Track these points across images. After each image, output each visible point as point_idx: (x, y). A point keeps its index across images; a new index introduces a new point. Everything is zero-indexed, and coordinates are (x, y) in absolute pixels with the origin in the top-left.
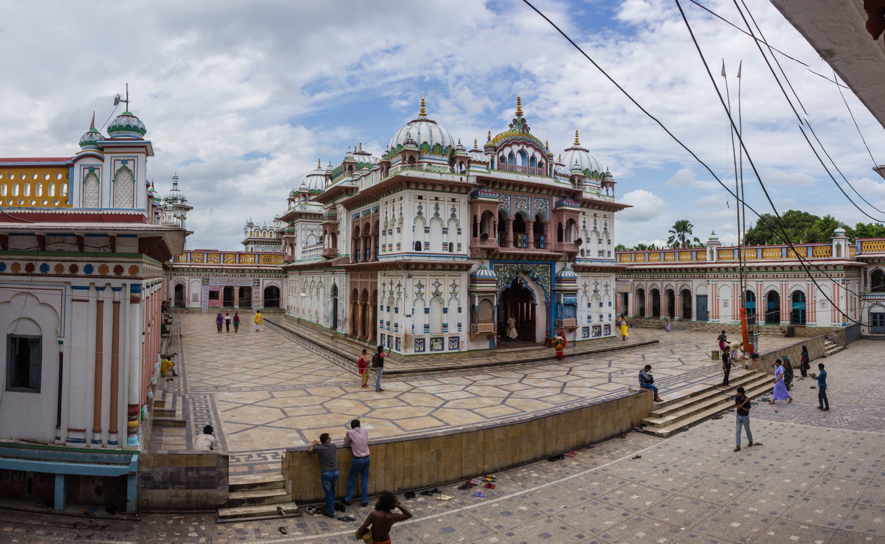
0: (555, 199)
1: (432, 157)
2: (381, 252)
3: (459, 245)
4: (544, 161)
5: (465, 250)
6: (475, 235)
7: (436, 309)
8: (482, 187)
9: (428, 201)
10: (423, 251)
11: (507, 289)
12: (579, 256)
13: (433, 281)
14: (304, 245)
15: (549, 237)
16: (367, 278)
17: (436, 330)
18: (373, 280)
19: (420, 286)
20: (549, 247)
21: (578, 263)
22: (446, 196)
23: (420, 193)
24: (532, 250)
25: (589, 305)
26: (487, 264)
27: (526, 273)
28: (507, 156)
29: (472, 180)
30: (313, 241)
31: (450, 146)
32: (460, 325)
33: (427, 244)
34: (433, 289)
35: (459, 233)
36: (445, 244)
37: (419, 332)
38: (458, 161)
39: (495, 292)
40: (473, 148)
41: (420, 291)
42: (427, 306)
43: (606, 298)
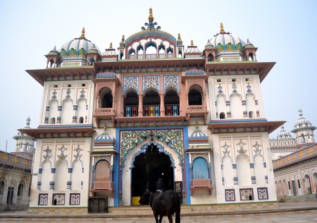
3: (86, 118)
4: (172, 47)
9: (61, 88)
11: (142, 154)
13: (60, 146)
19: (48, 150)
31: (83, 49)
33: (59, 119)
34: (59, 153)
35: (87, 109)
36: (75, 118)
37: (46, 188)
40: (108, 48)
41: (47, 155)
42: (53, 167)
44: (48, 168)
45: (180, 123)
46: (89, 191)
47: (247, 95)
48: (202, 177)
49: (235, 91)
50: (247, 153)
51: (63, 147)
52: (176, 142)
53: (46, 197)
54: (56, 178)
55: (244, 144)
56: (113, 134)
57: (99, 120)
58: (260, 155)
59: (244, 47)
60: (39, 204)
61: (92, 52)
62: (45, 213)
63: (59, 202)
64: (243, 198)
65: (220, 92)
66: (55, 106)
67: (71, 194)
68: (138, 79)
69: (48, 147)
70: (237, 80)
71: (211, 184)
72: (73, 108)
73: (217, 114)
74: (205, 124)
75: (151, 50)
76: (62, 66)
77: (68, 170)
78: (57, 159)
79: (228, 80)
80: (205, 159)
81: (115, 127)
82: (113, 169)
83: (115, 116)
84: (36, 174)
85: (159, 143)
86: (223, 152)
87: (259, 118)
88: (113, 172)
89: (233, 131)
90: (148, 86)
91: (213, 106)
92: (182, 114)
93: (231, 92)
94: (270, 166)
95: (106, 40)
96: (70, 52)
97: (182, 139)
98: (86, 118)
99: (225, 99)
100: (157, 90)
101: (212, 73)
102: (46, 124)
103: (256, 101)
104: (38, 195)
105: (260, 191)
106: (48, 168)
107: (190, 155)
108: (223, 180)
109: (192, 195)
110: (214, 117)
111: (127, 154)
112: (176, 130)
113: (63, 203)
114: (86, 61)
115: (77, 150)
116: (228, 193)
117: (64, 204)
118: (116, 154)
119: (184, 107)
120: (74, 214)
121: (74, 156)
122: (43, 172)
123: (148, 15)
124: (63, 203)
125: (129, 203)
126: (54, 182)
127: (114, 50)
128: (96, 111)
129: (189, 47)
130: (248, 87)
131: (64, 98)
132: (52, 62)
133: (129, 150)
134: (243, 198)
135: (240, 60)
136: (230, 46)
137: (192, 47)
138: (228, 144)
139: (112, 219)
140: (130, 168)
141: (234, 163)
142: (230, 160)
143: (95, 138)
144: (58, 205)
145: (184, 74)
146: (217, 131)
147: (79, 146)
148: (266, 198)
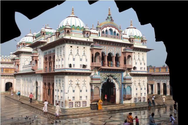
0: (123, 48)
1: (76, 31)
2: (55, 68)
4: (119, 33)
5: (89, 67)
6: (92, 61)
7: (77, 90)
8: (95, 43)
10: (72, 68)
11: (105, 82)
12: (132, 70)
14: (23, 65)
15: (121, 62)
16: (50, 78)
17: (77, 99)
18: (53, 79)
20: (121, 66)
21: (132, 72)
22: (81, 47)
23: (71, 45)
24: (114, 68)
25: (137, 89)
26: (97, 73)
27: (112, 76)
28: (105, 31)
29: (92, 41)
30: (27, 63)
31: (83, 27)
32: (86, 97)
38: (86, 33)
39: (100, 84)
41: (71, 84)
42: (74, 90)
43: (144, 86)
48: (129, 94)
49: (139, 58)
58: (144, 85)
60: (69, 107)
72: (80, 60)
84: (67, 93)
93: (138, 59)
103: (144, 63)
106: (71, 90)
113: (79, 106)
126: (74, 97)
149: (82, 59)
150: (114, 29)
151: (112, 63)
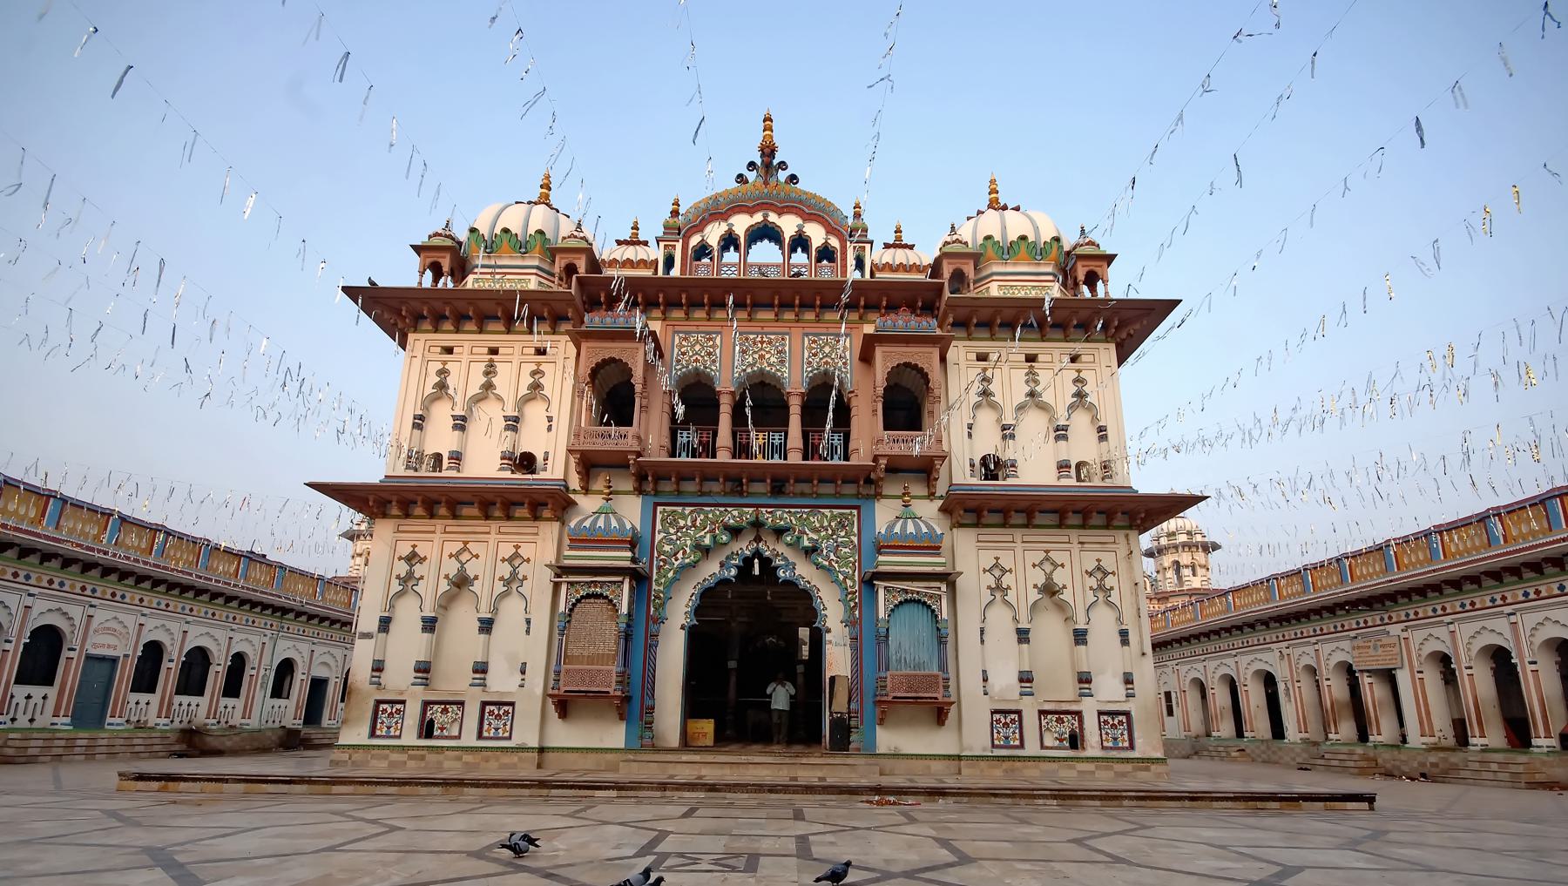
3: (546, 459)
4: (834, 242)
9: (465, 358)
11: (724, 582)
31: (540, 232)
33: (457, 457)
34: (452, 568)
35: (550, 428)
41: (410, 575)
42: (429, 613)
44: (409, 615)
45: (849, 489)
46: (546, 695)
47: (1071, 407)
48: (917, 666)
49: (1032, 394)
50: (1066, 596)
51: (465, 549)
52: (836, 550)
53: (398, 711)
54: (436, 649)
55: (1055, 565)
56: (631, 511)
57: (590, 464)
59: (1068, 253)
60: (373, 734)
61: (572, 243)
62: (392, 765)
63: (442, 729)
64: (1049, 740)
65: (985, 393)
66: (442, 415)
67: (484, 704)
68: (718, 341)
69: (414, 546)
70: (1041, 358)
71: (946, 687)
73: (972, 465)
74: (931, 496)
75: (765, 253)
76: (470, 282)
77: (478, 624)
78: (444, 586)
79: (1012, 357)
80: (929, 607)
81: (639, 491)
82: (628, 626)
83: (639, 454)
84: (368, 636)
85: (781, 548)
86: (989, 587)
87: (1108, 483)
88: (627, 636)
89: (1025, 521)
90: (752, 365)
91: (962, 436)
92: (861, 456)
93: (1021, 398)
94: (1142, 636)
95: (622, 211)
96: (498, 241)
97: (855, 539)
98: (546, 459)
99: (999, 420)
100: (778, 379)
101: (962, 333)
102: (411, 473)
103: (1101, 429)
104: (372, 704)
105: (1106, 722)
106: (409, 615)
107: (881, 593)
108: (986, 680)
109: (881, 722)
110: (961, 473)
111: (675, 579)
112: (836, 511)
113: (456, 733)
114: (553, 275)
115: (510, 560)
116: (998, 721)
117: (458, 737)
118: (640, 579)
119: (869, 437)
120: (492, 770)
121: (502, 579)
122: (392, 627)
123: (758, 137)
124: (456, 733)
125: (673, 737)
127: (646, 243)
128: (577, 435)
129: (887, 246)
130: (1077, 381)
131: (474, 389)
132: (438, 272)
133: (683, 567)
134: (1049, 741)
135: (1056, 291)
136: (1023, 245)
137: (898, 245)
138: (1006, 563)
139: (613, 793)
140: (683, 627)
141: (1024, 625)
142: (1007, 614)
143: (572, 525)
144: (438, 737)
145: (869, 329)
146: (970, 518)
147: (517, 547)
148: (1126, 744)
149: (516, 420)
150: (789, 225)
151: (777, 439)
